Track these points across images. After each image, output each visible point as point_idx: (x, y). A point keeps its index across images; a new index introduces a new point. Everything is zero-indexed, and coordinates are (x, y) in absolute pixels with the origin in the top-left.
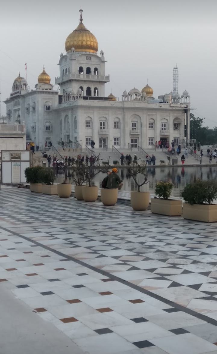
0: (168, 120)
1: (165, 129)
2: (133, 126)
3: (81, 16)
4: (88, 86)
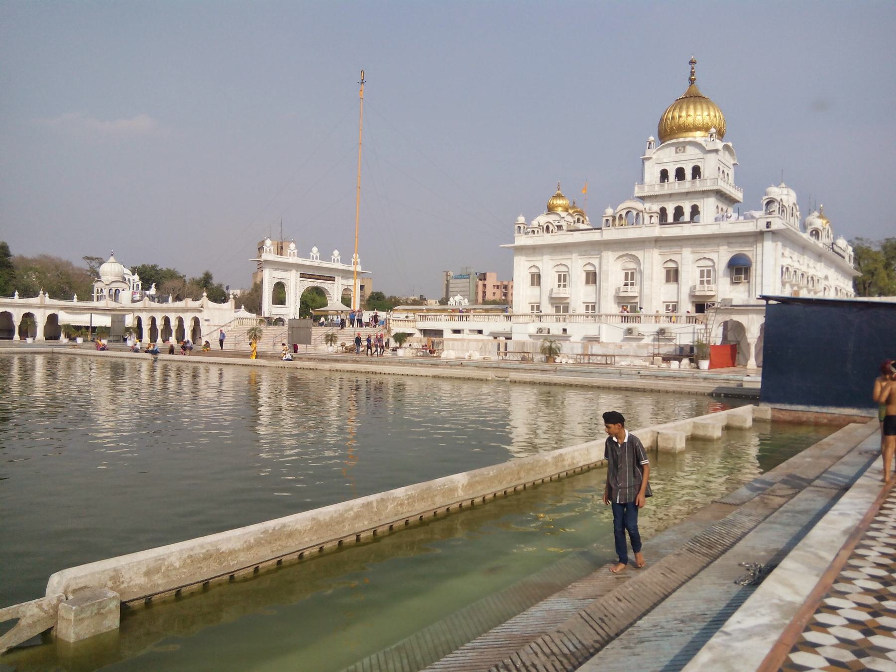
0: (716, 261)
1: (632, 284)
2: (626, 279)
3: (692, 74)
4: (676, 205)
